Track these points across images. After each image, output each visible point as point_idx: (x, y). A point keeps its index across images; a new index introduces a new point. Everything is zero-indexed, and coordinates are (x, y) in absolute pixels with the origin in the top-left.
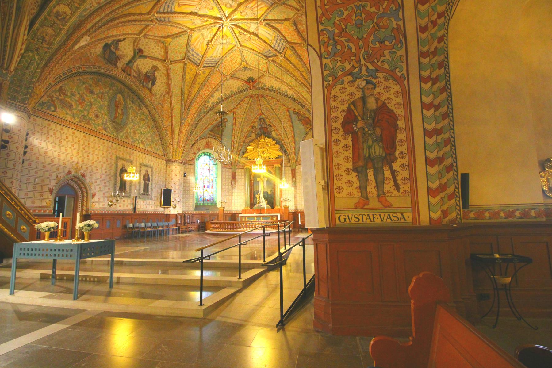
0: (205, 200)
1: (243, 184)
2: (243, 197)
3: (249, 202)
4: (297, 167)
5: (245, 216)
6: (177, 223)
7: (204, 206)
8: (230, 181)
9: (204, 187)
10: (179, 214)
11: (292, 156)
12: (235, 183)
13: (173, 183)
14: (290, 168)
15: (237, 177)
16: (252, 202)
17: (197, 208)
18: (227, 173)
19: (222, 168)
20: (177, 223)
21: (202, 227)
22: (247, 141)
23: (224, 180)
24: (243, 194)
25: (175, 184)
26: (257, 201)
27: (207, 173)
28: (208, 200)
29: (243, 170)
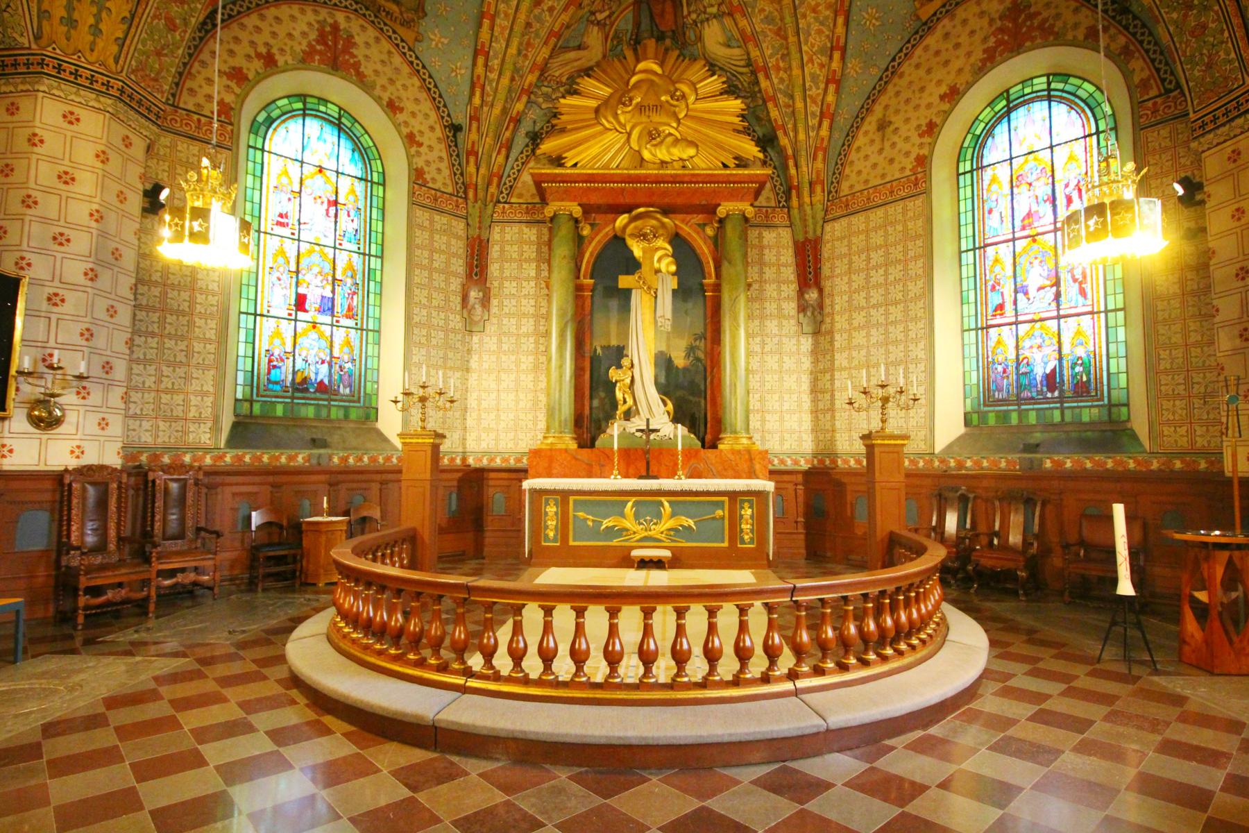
0: (301, 386)
1: (528, 306)
2: (527, 380)
3: (567, 408)
4: (835, 229)
5: (564, 495)
6: (62, 546)
7: (293, 421)
8: (456, 284)
9: (301, 302)
10: (86, 472)
11: (805, 170)
12: (485, 302)
13: (37, 233)
14: (785, 235)
15: (493, 269)
16: (593, 403)
17: (246, 429)
18: (440, 241)
19: (413, 202)
20: (62, 546)
21: (279, 560)
22: (559, 70)
23: (420, 276)
24: (527, 361)
25: (60, 240)
26: (615, 406)
27: (318, 225)
28: (321, 387)
29: (531, 233)
